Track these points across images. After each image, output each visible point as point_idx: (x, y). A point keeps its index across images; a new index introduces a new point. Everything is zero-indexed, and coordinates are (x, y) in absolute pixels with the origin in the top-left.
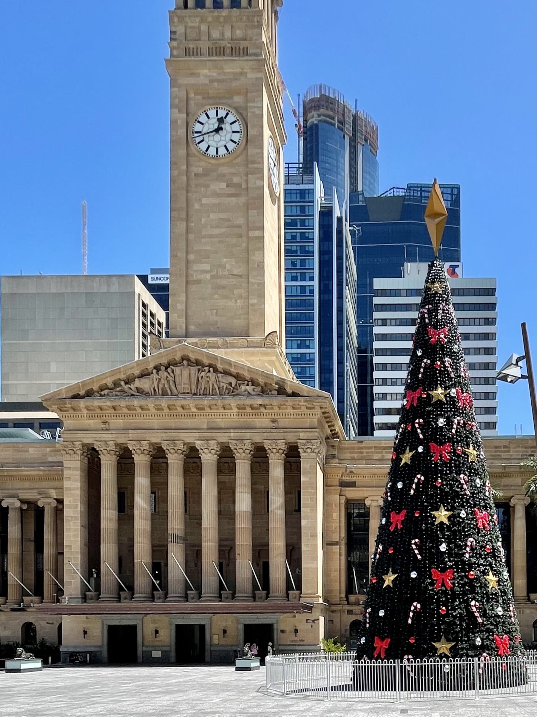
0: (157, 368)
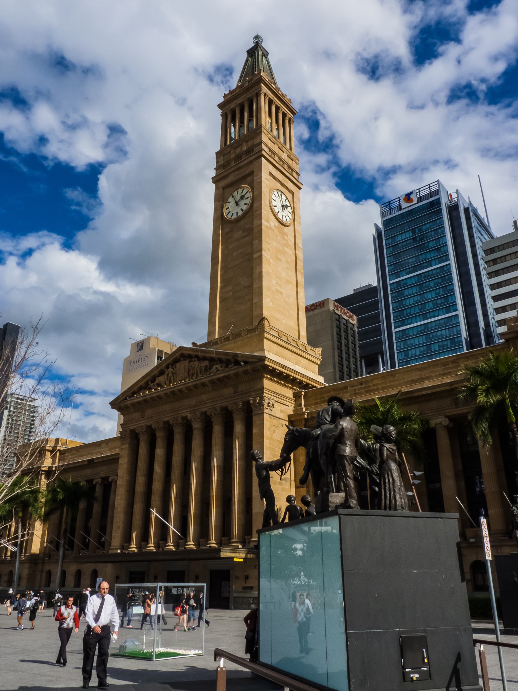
0: (167, 367)
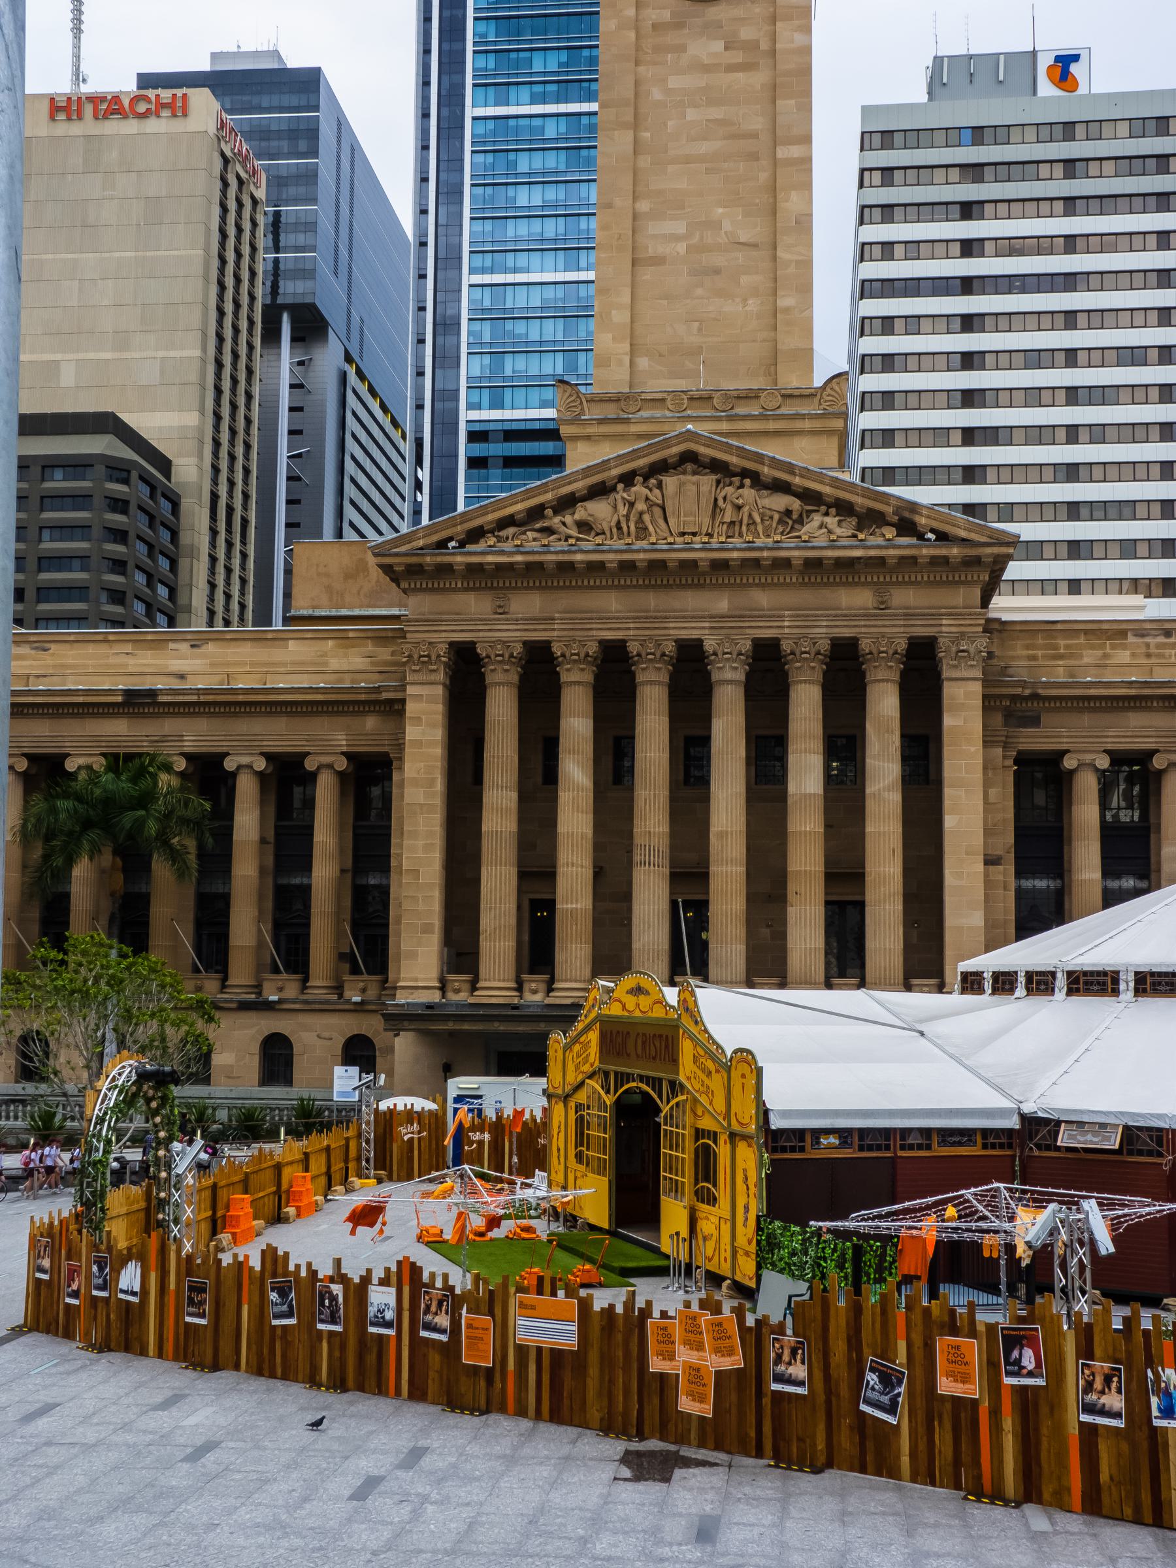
0: (628, 479)
